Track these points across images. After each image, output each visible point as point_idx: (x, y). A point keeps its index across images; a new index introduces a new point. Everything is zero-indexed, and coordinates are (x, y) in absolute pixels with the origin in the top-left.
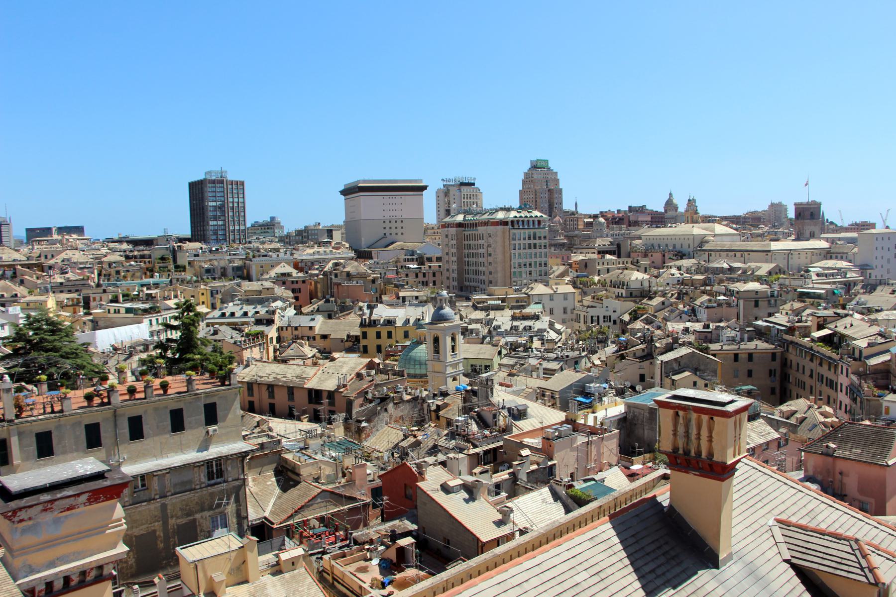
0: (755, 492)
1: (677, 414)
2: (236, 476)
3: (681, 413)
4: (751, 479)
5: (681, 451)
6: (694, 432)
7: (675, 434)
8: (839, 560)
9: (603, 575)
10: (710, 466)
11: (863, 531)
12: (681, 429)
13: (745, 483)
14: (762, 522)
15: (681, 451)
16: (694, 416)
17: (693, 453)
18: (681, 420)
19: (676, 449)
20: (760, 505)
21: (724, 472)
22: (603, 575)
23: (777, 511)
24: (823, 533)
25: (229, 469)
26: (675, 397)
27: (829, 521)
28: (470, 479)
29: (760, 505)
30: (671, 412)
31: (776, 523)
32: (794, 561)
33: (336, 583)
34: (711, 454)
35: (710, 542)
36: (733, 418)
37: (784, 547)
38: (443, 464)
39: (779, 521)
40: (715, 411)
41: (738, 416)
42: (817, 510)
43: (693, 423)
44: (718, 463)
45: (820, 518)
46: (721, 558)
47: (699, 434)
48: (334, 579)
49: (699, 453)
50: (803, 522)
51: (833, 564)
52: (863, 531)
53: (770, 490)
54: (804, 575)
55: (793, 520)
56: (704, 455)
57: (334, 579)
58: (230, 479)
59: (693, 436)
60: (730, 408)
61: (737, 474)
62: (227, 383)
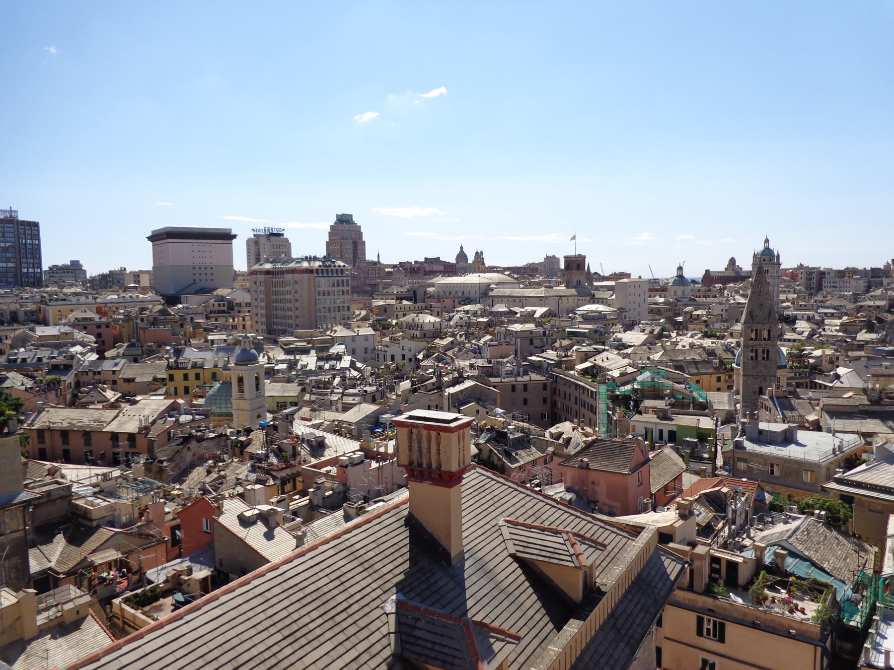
0: (488, 498)
1: (411, 432)
2: (16, 528)
3: (414, 430)
4: (487, 486)
5: (415, 464)
6: (424, 445)
7: (410, 450)
8: (552, 550)
9: (343, 579)
10: (440, 475)
11: (580, 526)
12: (415, 445)
13: (480, 490)
14: (493, 523)
15: (415, 464)
16: (424, 432)
17: (425, 465)
18: (414, 437)
19: (411, 463)
20: (493, 508)
21: (452, 479)
22: (343, 579)
23: (507, 513)
24: (543, 530)
25: (7, 520)
26: (411, 417)
27: (552, 519)
28: (265, 508)
29: (493, 508)
30: (406, 430)
31: (505, 523)
32: (519, 554)
33: (126, 627)
34: (439, 466)
35: (443, 542)
36: (457, 433)
37: (510, 544)
38: (241, 496)
39: (507, 521)
40: (441, 429)
41: (461, 431)
42: (543, 510)
43: (424, 439)
44: (445, 472)
45: (544, 517)
46: (453, 554)
47: (429, 448)
48: (124, 623)
49: (430, 466)
50: (529, 522)
51: (548, 554)
52: (580, 526)
53: (502, 495)
54: (527, 567)
55: (521, 520)
56: (434, 465)
57: (124, 623)
58: (8, 531)
59: (424, 451)
60: (452, 425)
61: (464, 482)
62: (6, 430)
